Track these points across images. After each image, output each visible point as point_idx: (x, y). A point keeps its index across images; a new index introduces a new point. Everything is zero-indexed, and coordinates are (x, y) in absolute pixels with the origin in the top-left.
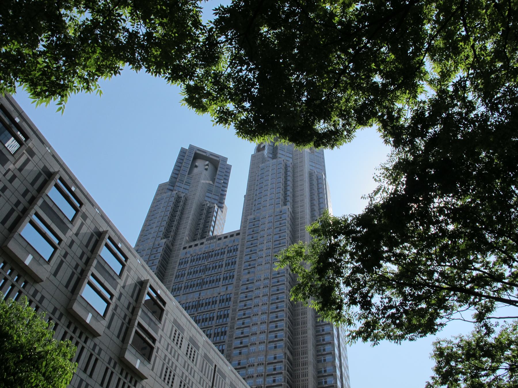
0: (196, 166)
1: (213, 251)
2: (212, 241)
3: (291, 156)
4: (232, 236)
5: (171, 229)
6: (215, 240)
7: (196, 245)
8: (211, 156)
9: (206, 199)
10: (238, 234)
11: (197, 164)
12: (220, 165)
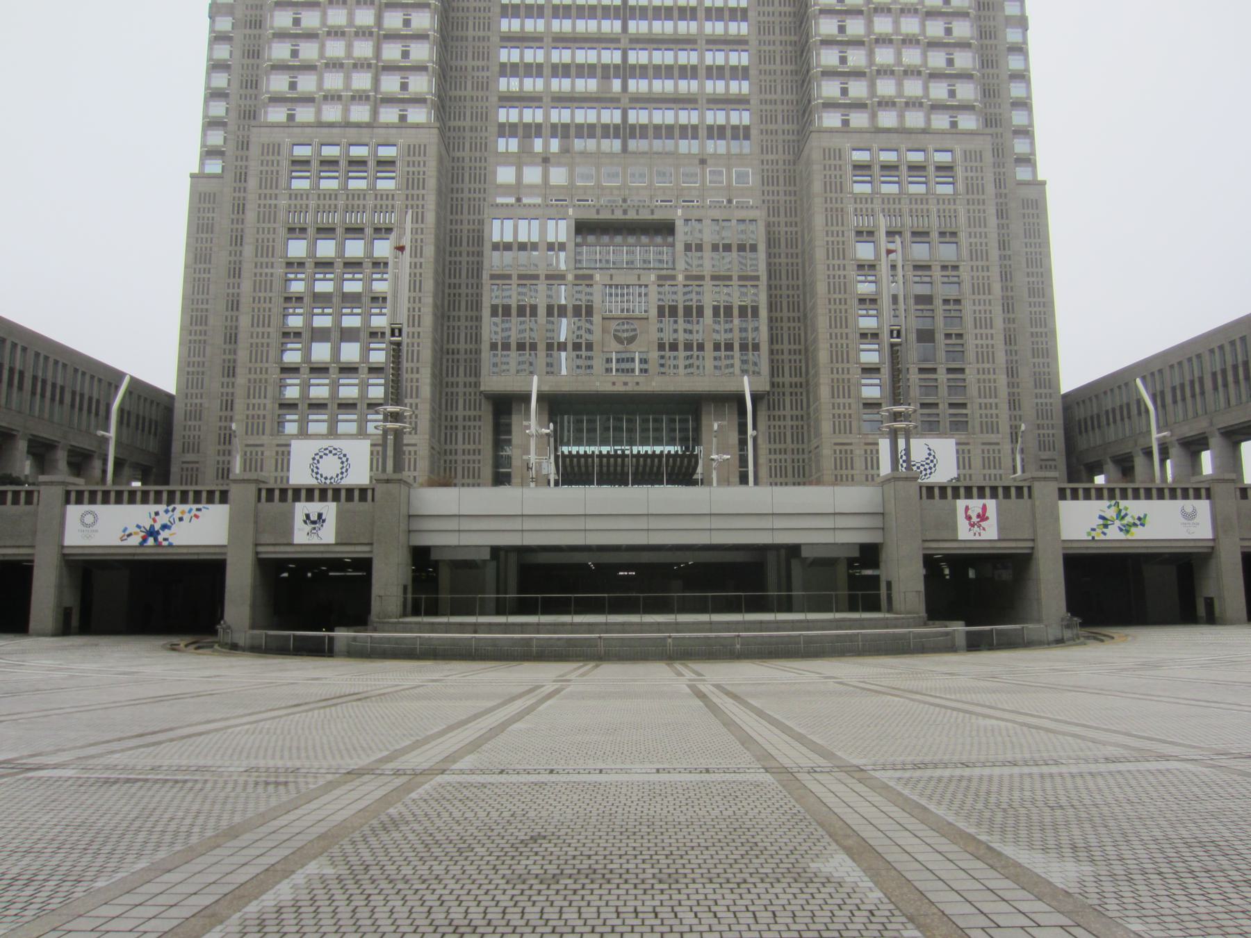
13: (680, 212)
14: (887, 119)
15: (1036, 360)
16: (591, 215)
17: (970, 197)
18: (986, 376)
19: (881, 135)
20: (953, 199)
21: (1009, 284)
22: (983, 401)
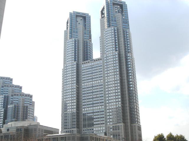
3: (115, 23)
4: (99, 60)
5: (76, 58)
7: (87, 63)
8: (82, 15)
9: (85, 38)
10: (101, 59)
11: (78, 20)
12: (86, 19)
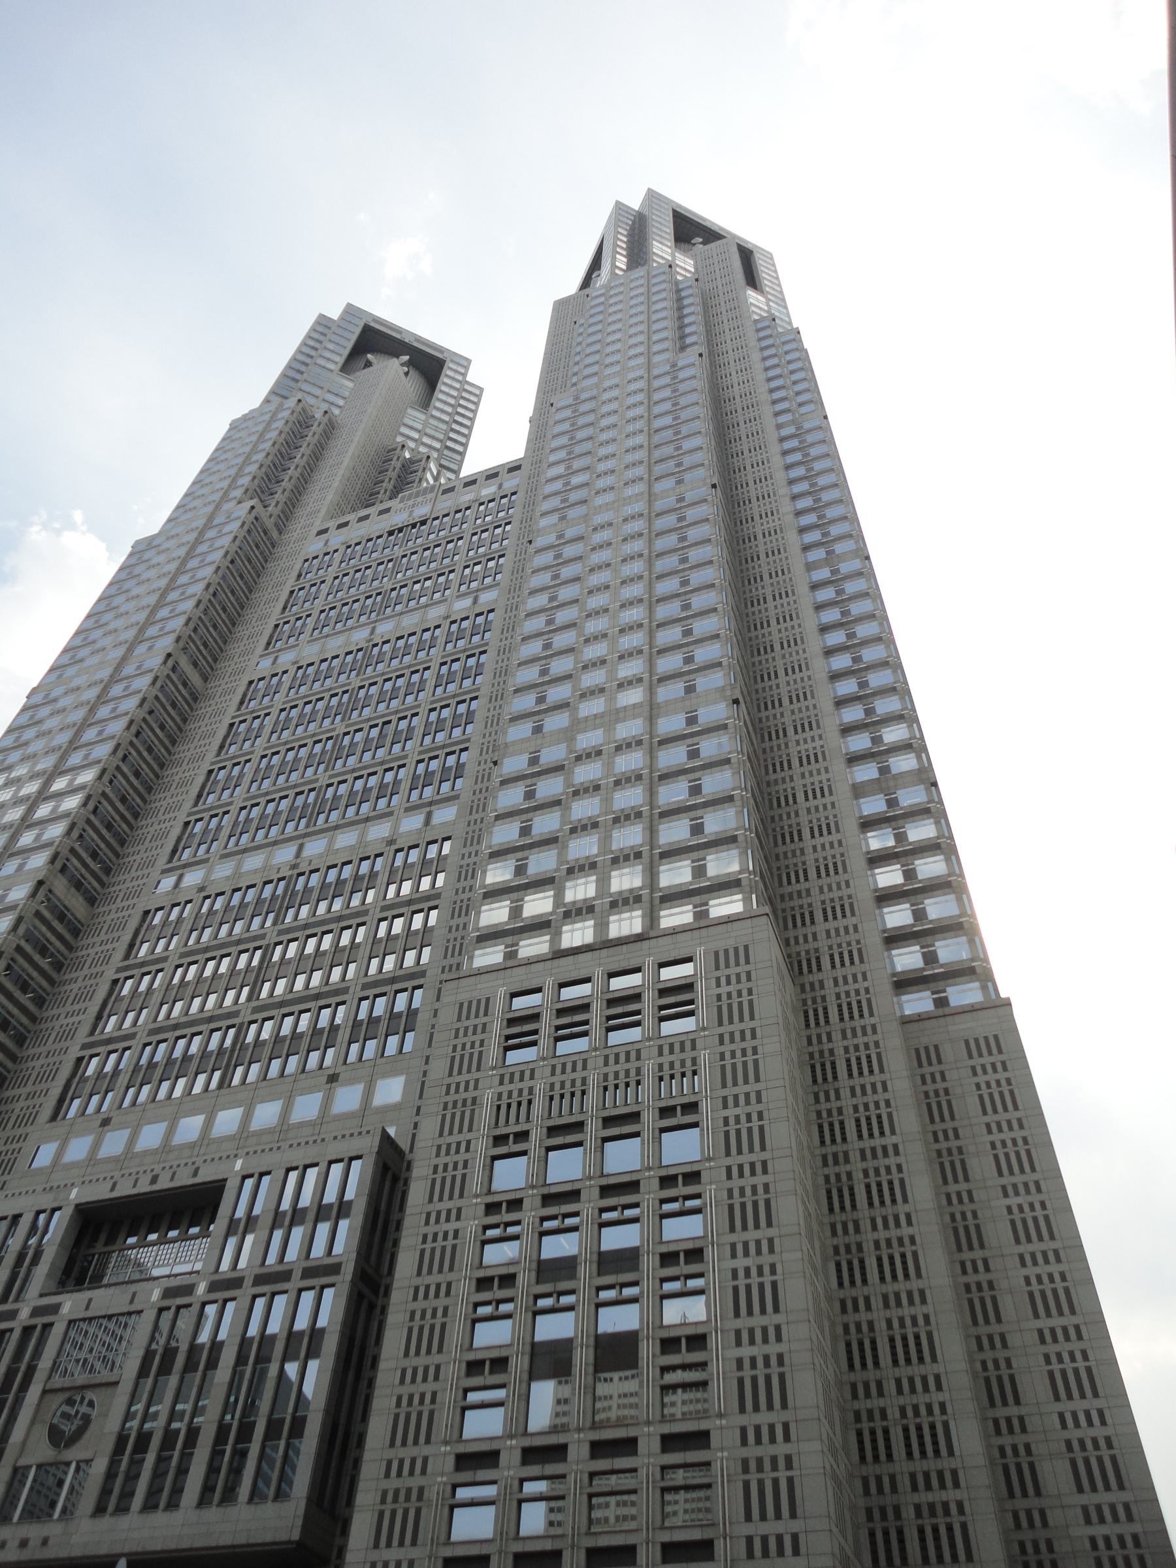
0: (368, 364)
1: (423, 523)
2: (420, 499)
6: (429, 496)
8: (415, 344)
12: (446, 371)
13: (238, 1164)
14: (578, 934)
15: (1066, 1406)
16: (100, 1192)
17: (726, 1029)
18: (766, 1450)
19: (563, 961)
20: (689, 1043)
21: (902, 1209)
22: (758, 1529)
